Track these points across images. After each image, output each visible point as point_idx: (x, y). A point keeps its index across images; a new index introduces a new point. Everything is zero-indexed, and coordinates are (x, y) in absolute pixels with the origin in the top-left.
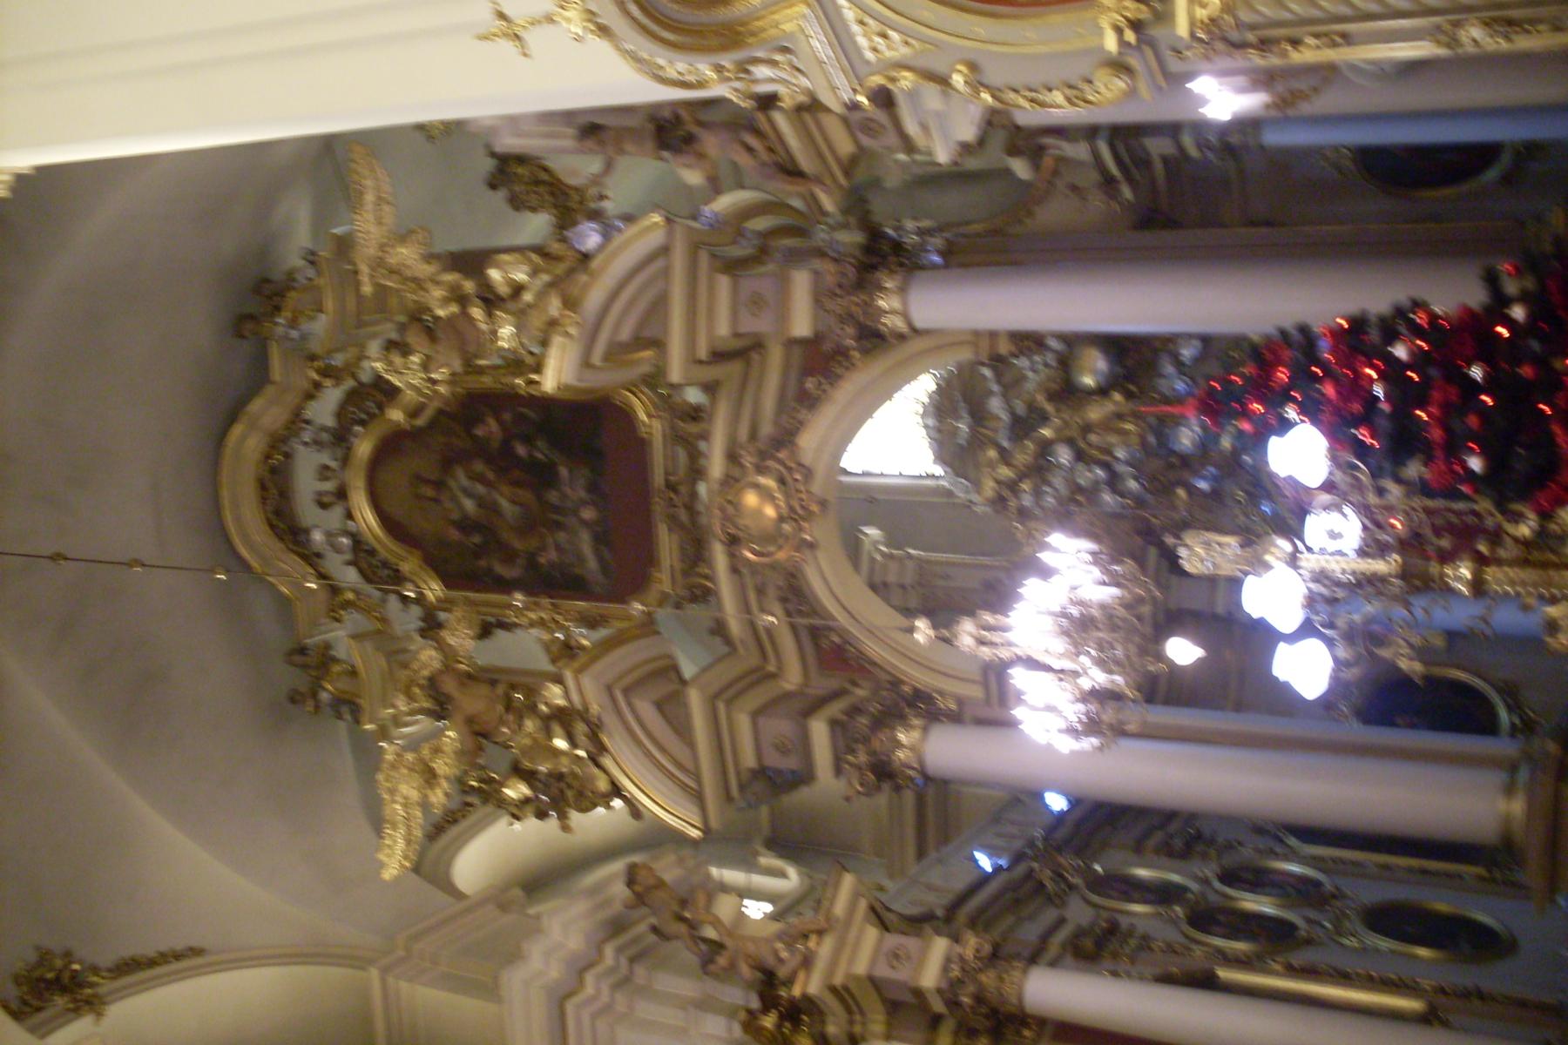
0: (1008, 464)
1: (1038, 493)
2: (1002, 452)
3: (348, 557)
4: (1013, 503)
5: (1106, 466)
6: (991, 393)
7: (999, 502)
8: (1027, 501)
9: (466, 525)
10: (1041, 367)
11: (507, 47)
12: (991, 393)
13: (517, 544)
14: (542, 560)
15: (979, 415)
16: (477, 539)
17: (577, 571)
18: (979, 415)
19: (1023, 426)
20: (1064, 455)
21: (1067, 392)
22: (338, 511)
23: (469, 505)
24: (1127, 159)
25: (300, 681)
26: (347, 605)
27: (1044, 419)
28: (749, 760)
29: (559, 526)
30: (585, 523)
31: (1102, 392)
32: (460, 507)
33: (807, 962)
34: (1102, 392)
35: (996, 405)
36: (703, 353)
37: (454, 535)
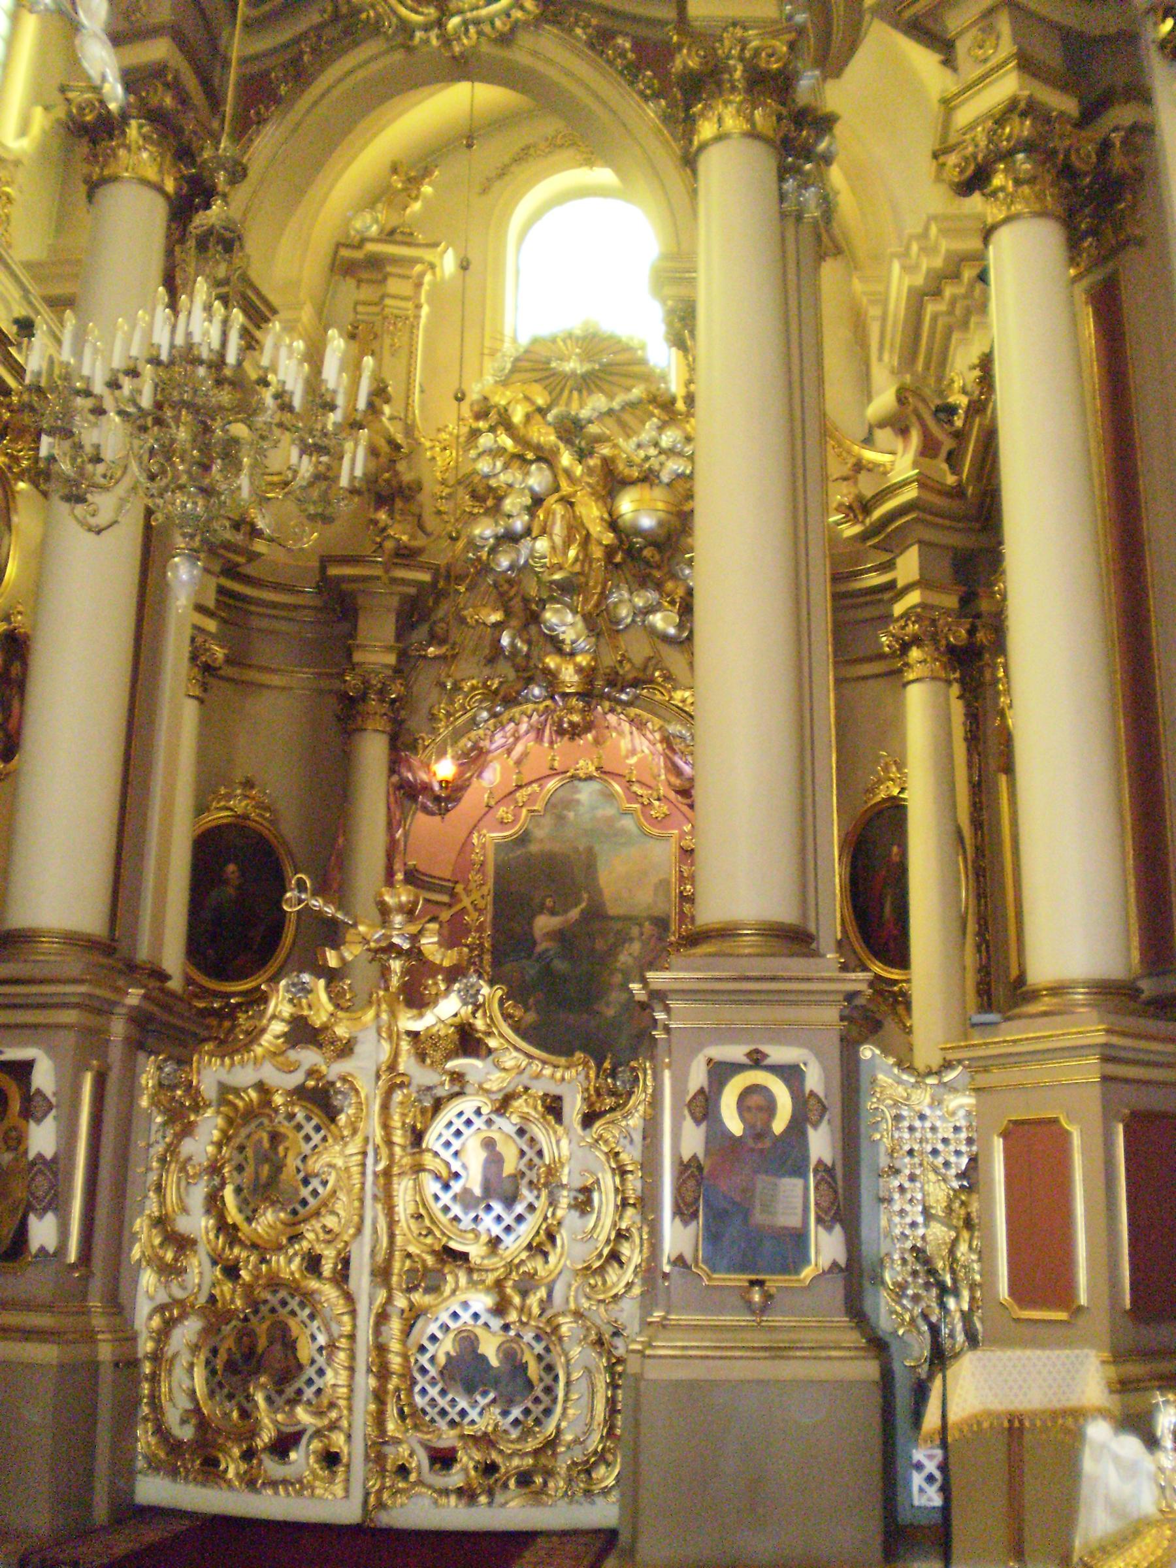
0: (528, 417)
1: (497, 452)
2: (542, 411)
4: (482, 425)
5: (528, 531)
6: (611, 397)
7: (487, 412)
8: (486, 441)
10: (642, 453)
12: (611, 397)
15: (587, 383)
18: (587, 383)
19: (570, 430)
20: (538, 479)
21: (612, 482)
27: (582, 455)
31: (613, 524)
34: (613, 524)
35: (598, 402)
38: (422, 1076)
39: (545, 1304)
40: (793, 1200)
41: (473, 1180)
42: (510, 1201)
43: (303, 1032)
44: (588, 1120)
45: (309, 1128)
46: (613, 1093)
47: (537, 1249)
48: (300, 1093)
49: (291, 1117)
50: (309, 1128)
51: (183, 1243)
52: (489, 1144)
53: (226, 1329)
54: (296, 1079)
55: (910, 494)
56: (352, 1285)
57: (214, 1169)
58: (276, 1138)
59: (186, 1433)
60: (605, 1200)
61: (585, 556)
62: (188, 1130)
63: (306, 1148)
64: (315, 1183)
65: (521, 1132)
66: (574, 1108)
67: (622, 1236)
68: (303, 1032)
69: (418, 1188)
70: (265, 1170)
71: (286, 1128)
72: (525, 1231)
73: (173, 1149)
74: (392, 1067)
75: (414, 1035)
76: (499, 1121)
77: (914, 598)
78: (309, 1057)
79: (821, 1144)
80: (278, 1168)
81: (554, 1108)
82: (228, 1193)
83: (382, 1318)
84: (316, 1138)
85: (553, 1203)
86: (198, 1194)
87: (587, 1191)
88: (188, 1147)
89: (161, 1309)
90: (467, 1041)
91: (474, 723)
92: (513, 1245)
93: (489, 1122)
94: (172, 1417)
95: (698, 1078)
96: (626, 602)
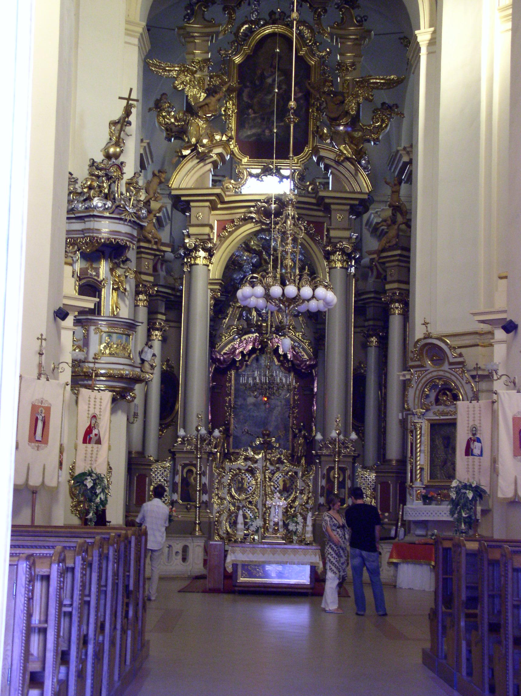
3: (249, 19)
9: (263, 78)
11: (423, 322)
13: (255, 100)
14: (250, 111)
16: (257, 82)
17: (247, 126)
22: (268, 18)
23: (269, 80)
24: (366, 301)
26: (230, 14)
28: (192, 204)
29: (263, 119)
30: (264, 131)
32: (268, 77)
36: (327, 201)
37: (259, 72)
38: (272, 468)
39: (294, 511)
41: (281, 487)
42: (288, 492)
43: (247, 459)
44: (303, 475)
45: (249, 477)
46: (307, 471)
47: (294, 501)
48: (247, 470)
49: (245, 475)
50: (249, 477)
52: (284, 481)
53: (233, 515)
54: (247, 467)
55: (372, 295)
56: (258, 507)
57: (229, 485)
58: (242, 479)
59: (225, 536)
62: (223, 477)
63: (249, 481)
64: (251, 488)
65: (290, 479)
66: (300, 474)
67: (309, 498)
68: (247, 459)
69: (271, 489)
70: (240, 485)
71: (244, 477)
73: (220, 481)
74: (266, 466)
76: (286, 477)
78: (249, 463)
80: (243, 484)
81: (296, 473)
82: (233, 489)
83: (265, 513)
84: (251, 479)
85: (296, 492)
86: (226, 490)
87: (302, 490)
88: (223, 480)
89: (218, 512)
90: (280, 461)
91: (234, 339)
93: (284, 477)
94: (221, 533)
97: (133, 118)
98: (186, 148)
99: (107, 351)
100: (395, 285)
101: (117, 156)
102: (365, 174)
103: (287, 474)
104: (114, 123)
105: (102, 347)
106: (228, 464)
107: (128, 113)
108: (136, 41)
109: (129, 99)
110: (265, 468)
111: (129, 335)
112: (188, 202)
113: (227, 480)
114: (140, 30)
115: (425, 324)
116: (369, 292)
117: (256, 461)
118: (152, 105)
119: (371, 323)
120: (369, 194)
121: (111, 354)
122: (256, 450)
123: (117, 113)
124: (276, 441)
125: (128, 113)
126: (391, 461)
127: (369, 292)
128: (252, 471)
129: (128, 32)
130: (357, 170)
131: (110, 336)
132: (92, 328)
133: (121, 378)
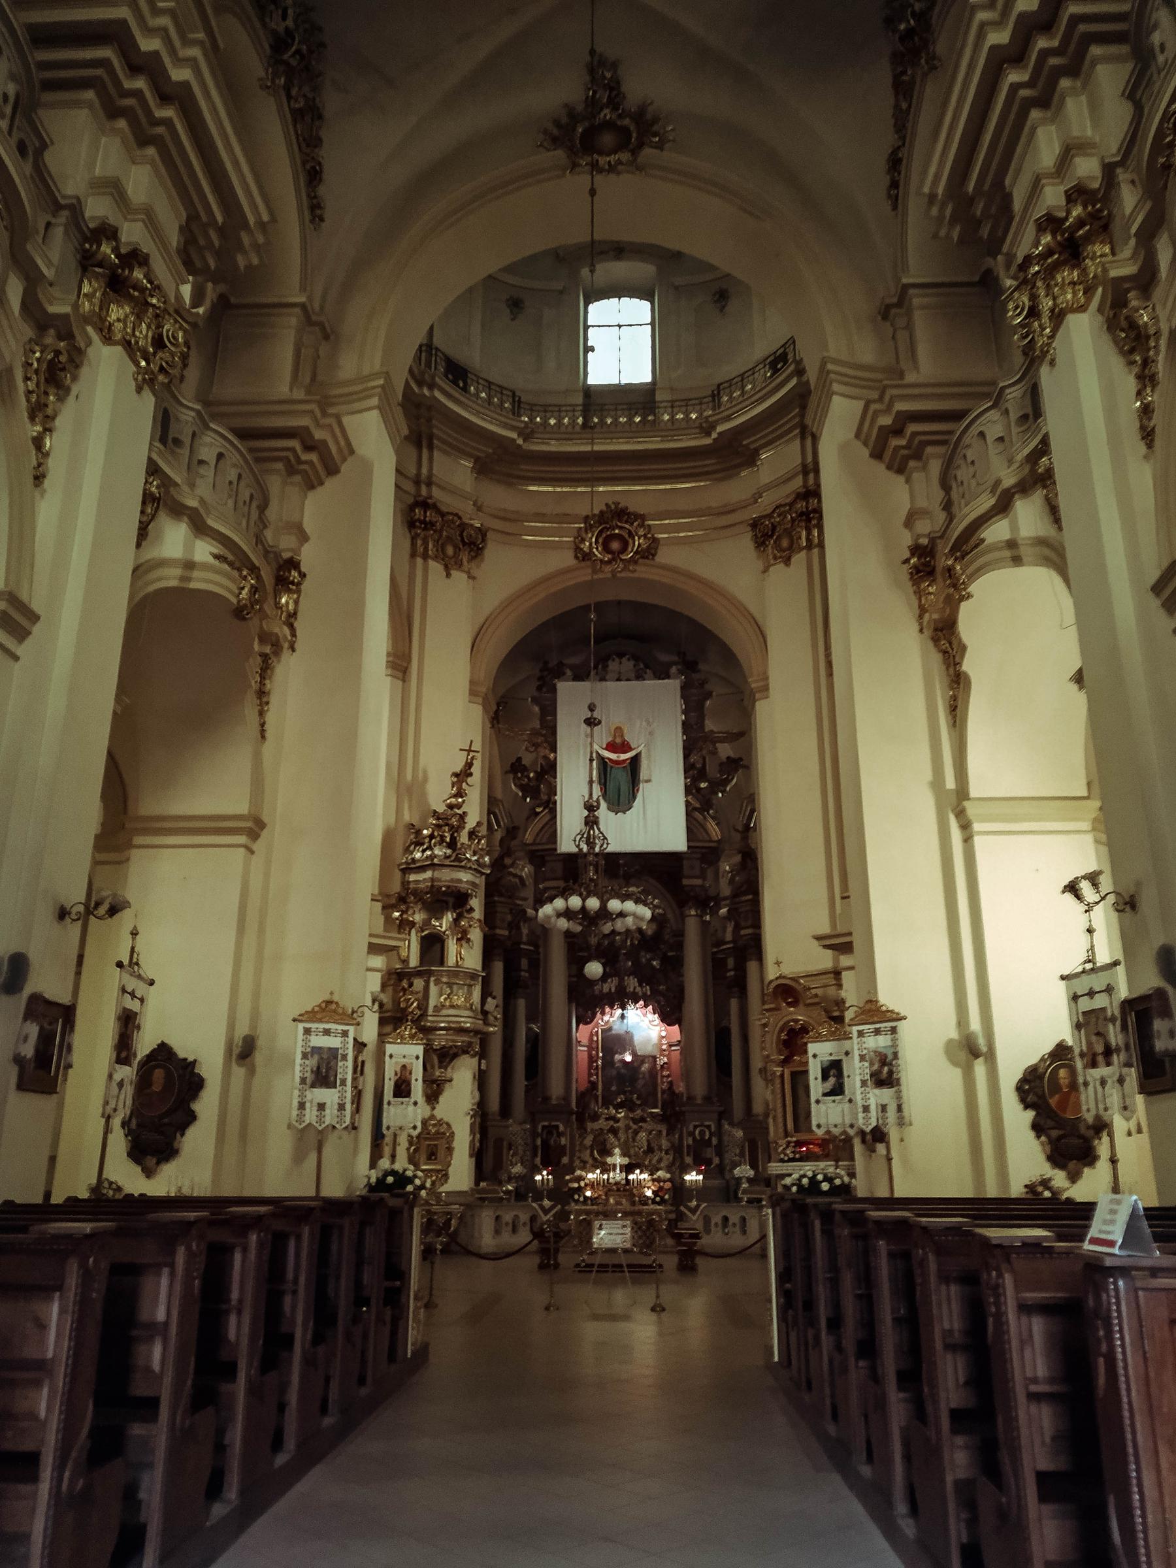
25: (553, 663)
33: (501, 895)
38: (635, 1127)
40: (710, 1153)
44: (667, 1135)
51: (585, 1162)
60: (671, 1152)
61: (632, 944)
66: (664, 1133)
72: (656, 1158)
75: (632, 1119)
77: (732, 973)
78: (611, 1123)
79: (714, 1141)
86: (588, 1151)
92: (654, 1161)
95: (691, 1128)
96: (644, 957)
97: (476, 769)
98: (539, 806)
99: (447, 1003)
100: (750, 931)
101: (459, 806)
102: (713, 823)
103: (650, 1133)
104: (456, 775)
105: (442, 999)
106: (590, 1126)
107: (469, 765)
108: (480, 700)
109: (469, 751)
110: (628, 1128)
111: (470, 986)
112: (543, 857)
113: (588, 1141)
114: (484, 690)
115: (778, 963)
116: (728, 942)
117: (617, 1121)
118: (509, 768)
119: (732, 973)
120: (719, 841)
121: (452, 1007)
122: (617, 1107)
123: (458, 767)
124: (638, 1098)
125: (469, 765)
126: (757, 1115)
127: (728, 942)
128: (614, 1131)
129: (473, 693)
130: (705, 818)
131: (451, 988)
132: (432, 979)
133: (462, 1031)
